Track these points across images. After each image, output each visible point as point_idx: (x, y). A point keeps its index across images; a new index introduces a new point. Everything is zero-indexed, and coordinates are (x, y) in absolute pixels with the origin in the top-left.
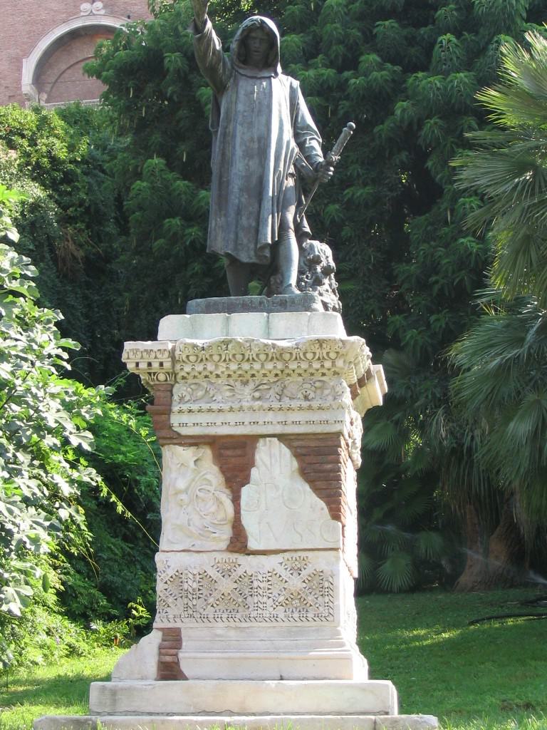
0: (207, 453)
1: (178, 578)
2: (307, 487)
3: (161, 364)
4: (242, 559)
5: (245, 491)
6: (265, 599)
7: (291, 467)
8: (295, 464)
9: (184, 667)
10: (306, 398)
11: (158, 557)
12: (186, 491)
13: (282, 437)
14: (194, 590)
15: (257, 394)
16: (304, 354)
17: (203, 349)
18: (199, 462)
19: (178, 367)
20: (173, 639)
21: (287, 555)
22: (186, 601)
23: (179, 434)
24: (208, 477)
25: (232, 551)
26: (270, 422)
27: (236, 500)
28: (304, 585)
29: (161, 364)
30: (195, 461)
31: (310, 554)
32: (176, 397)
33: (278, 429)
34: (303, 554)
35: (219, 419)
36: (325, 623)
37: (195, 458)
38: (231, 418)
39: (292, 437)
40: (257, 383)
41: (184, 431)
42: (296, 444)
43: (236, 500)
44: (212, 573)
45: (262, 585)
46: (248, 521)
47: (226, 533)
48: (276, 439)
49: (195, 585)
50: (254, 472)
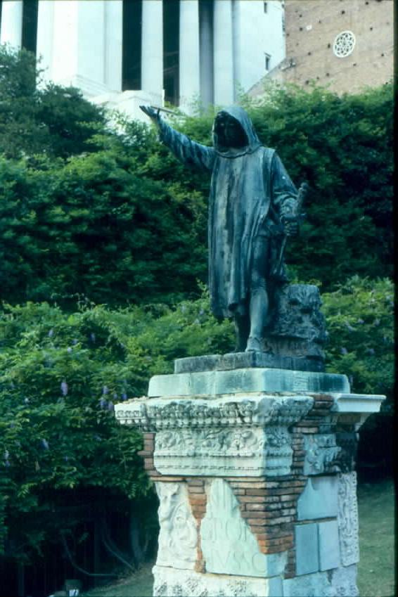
0: (184, 487)
3: (140, 420)
4: (204, 578)
7: (232, 504)
8: (235, 501)
16: (228, 412)
17: (161, 410)
18: (177, 496)
19: (153, 422)
23: (160, 474)
27: (198, 529)
29: (140, 420)
30: (174, 495)
31: (248, 581)
32: (156, 445)
33: (223, 473)
39: (232, 479)
40: (206, 432)
41: (163, 472)
42: (235, 485)
43: (198, 529)
48: (221, 481)
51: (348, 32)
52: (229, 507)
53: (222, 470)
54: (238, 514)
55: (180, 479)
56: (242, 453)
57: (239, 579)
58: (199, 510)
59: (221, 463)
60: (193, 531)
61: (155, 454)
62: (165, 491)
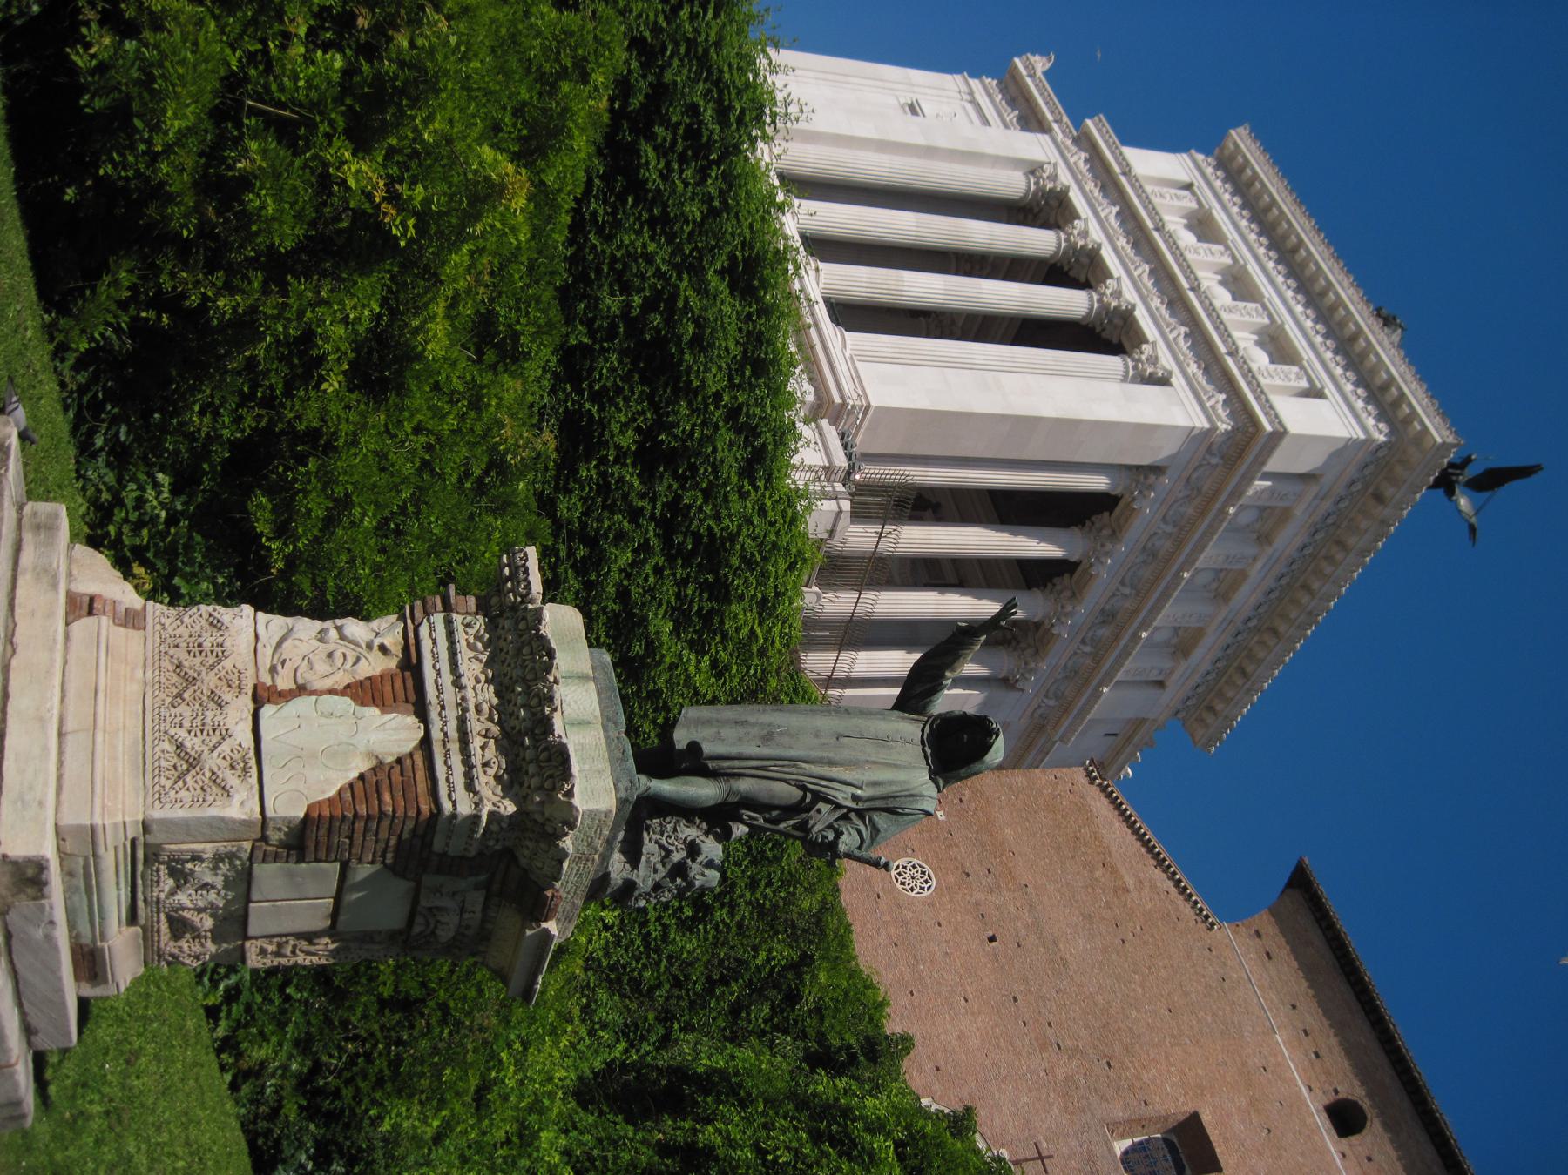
1: (217, 625)
2: (354, 774)
4: (246, 703)
5: (346, 703)
6: (187, 724)
8: (389, 759)
9: (83, 625)
10: (486, 765)
11: (247, 609)
12: (343, 637)
13: (426, 743)
14: (200, 645)
15: (486, 707)
16: (546, 749)
20: (132, 620)
21: (252, 753)
22: (186, 636)
24: (363, 661)
25: (255, 686)
26: (444, 724)
27: (332, 692)
28: (208, 774)
31: (254, 780)
32: (469, 619)
33: (436, 735)
34: (254, 771)
35: (445, 666)
36: (150, 800)
37: (387, 643)
38: (447, 678)
41: (424, 630)
44: (228, 664)
45: (208, 720)
46: (303, 704)
47: (284, 683)
49: (207, 645)
50: (373, 711)
51: (934, 883)
52: (379, 750)
53: (441, 735)
54: (373, 763)
55: (414, 661)
56: (478, 772)
57: (253, 763)
58: (366, 692)
59: (453, 733)
60: (327, 684)
61: (454, 616)
62: (388, 629)
